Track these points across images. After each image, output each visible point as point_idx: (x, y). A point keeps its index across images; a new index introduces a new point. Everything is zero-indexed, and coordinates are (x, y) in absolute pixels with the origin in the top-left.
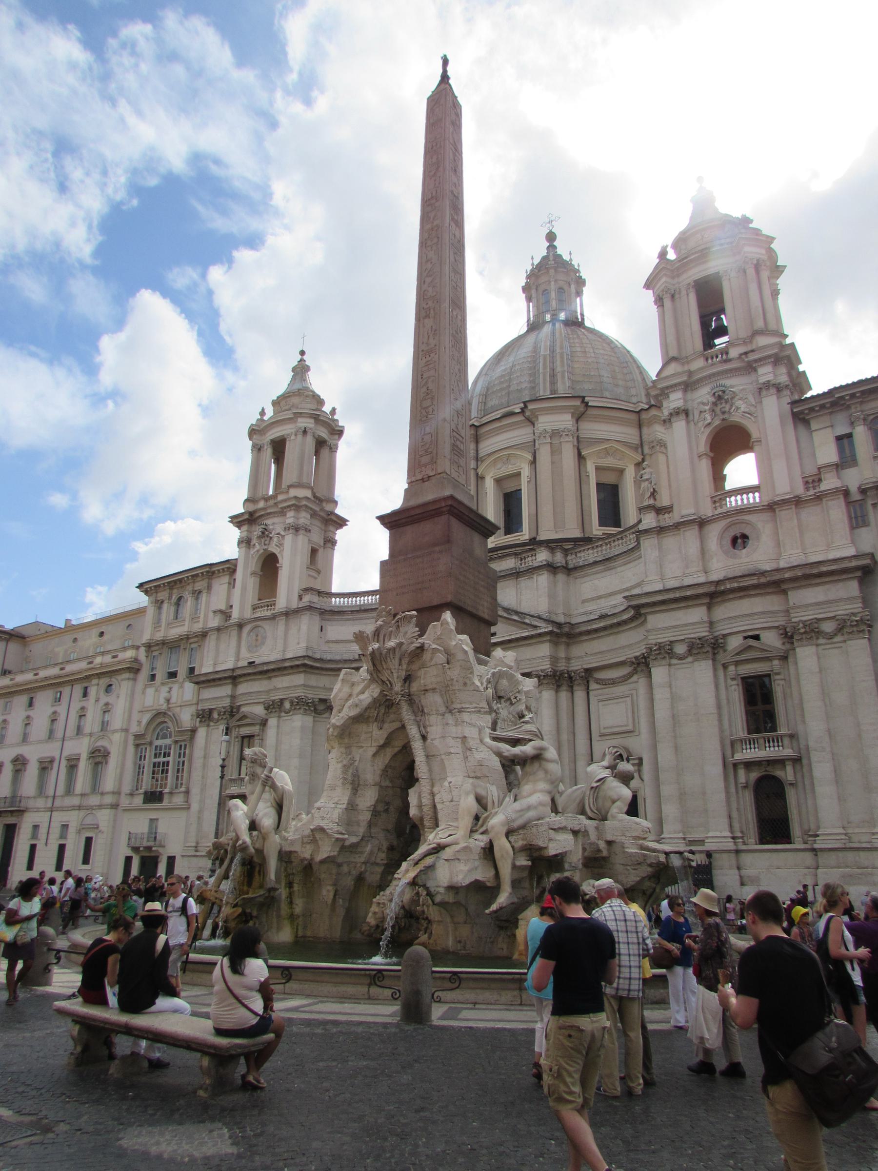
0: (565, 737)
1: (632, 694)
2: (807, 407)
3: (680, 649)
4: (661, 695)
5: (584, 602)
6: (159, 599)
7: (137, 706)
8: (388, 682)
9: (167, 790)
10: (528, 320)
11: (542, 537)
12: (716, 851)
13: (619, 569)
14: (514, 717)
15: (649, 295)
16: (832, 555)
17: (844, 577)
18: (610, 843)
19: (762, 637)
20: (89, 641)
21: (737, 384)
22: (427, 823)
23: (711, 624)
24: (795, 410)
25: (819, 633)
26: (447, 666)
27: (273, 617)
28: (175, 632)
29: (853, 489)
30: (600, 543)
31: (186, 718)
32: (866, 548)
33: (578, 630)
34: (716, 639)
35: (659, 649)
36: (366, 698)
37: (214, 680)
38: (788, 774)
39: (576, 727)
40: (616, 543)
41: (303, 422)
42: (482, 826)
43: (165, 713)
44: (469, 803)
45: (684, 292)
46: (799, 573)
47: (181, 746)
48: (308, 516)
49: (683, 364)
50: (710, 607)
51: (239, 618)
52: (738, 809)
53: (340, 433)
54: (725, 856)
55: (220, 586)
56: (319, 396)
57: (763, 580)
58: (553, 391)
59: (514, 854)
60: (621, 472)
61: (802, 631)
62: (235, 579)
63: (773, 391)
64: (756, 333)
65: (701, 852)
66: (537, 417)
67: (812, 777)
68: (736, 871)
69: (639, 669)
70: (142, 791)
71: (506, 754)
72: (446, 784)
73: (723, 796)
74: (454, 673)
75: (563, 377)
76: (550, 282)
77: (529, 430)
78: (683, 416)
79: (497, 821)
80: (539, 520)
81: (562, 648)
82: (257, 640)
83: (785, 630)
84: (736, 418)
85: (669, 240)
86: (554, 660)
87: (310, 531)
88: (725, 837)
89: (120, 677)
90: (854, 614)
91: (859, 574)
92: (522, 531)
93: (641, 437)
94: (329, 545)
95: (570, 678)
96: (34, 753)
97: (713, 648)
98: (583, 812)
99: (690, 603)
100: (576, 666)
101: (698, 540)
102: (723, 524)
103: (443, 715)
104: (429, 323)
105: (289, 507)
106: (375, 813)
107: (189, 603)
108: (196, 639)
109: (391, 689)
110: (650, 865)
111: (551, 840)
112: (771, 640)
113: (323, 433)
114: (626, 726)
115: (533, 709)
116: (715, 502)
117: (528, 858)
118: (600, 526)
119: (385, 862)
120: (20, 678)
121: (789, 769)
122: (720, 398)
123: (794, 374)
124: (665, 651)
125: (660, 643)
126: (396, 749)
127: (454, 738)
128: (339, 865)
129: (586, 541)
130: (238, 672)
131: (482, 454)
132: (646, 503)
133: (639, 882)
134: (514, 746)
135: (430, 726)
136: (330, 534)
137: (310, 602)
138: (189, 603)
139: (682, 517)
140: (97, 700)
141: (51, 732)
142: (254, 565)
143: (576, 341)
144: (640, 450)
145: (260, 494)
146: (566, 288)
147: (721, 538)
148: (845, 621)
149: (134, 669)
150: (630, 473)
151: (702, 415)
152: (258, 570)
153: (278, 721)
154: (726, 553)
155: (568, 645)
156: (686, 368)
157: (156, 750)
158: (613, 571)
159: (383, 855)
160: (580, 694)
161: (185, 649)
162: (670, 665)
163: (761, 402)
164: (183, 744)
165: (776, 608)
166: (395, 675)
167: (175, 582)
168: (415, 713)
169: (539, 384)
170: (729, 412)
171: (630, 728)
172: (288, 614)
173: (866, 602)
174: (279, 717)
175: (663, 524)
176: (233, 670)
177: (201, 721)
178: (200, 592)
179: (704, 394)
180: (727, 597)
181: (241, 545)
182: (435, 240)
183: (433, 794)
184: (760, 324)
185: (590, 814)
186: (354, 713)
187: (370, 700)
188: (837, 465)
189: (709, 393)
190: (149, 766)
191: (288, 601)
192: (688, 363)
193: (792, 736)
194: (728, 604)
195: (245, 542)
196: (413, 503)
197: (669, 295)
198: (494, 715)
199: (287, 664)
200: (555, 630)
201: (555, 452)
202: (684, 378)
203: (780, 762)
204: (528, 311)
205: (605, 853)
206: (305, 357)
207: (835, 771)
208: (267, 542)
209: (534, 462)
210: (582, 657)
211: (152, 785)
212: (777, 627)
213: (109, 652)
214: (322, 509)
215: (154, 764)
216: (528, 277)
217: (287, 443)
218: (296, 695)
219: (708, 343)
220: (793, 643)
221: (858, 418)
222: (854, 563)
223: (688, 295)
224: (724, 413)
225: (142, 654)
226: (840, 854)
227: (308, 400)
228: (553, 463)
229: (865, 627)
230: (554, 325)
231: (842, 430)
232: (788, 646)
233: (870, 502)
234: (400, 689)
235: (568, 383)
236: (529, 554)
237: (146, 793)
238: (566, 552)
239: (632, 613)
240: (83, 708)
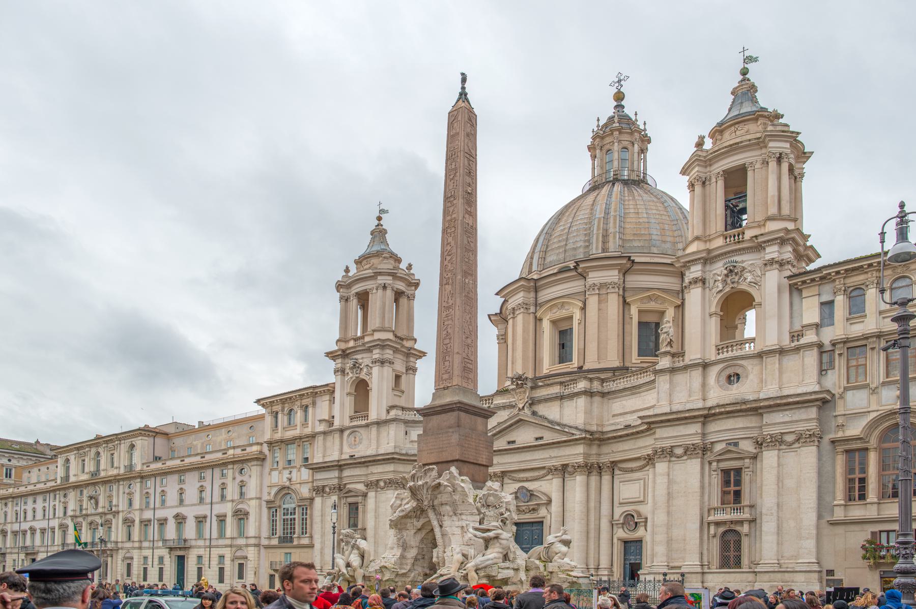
108: (307, 439)
129: (623, 370)
134: (484, 533)
161: (299, 446)
213: (238, 447)
225: (265, 449)
236: (572, 382)
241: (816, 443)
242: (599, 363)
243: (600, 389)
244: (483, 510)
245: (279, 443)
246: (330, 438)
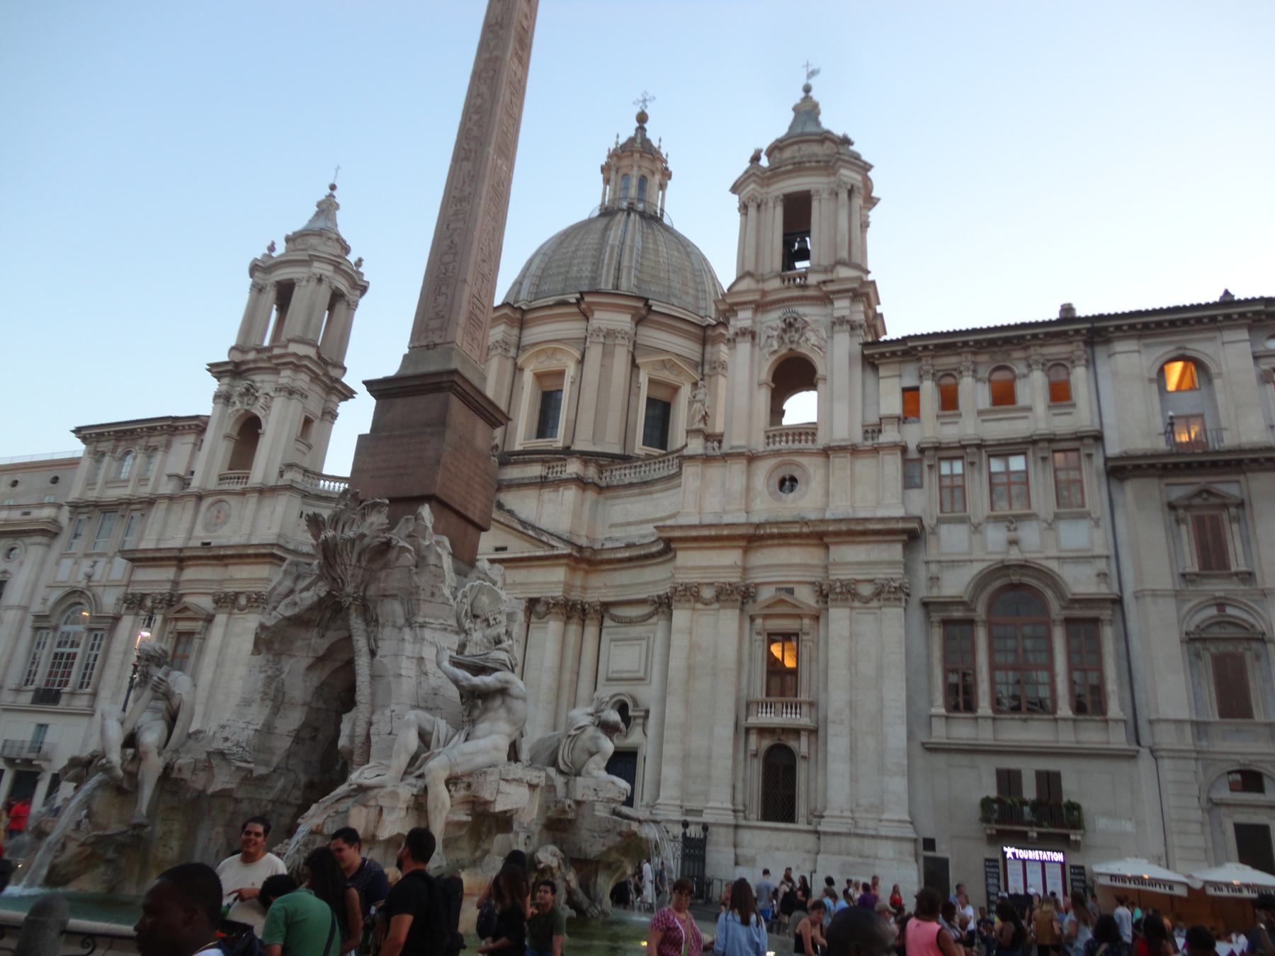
1: (649, 638)
2: (878, 351)
3: (708, 593)
4: (679, 641)
5: (612, 526)
6: (100, 449)
8: (339, 581)
9: (67, 689)
10: (603, 203)
11: (578, 446)
12: (714, 824)
13: (655, 496)
14: (490, 642)
15: (734, 200)
16: (880, 513)
17: (889, 538)
18: (579, 803)
21: (809, 312)
22: (356, 758)
23: (745, 570)
24: (865, 352)
25: (855, 595)
26: (414, 570)
27: (243, 493)
28: (113, 494)
29: (912, 446)
30: (639, 463)
31: (109, 601)
32: (916, 511)
33: (599, 557)
34: (747, 587)
35: (685, 590)
36: (309, 597)
37: (154, 559)
38: (802, 746)
39: (583, 666)
40: (657, 466)
41: (319, 268)
42: (420, 767)
43: (82, 592)
44: (411, 741)
45: (771, 204)
46: (844, 527)
47: (96, 636)
48: (307, 379)
49: (758, 281)
50: (746, 551)
51: (199, 488)
52: (744, 780)
53: (363, 289)
54: (722, 831)
55: (182, 446)
56: (345, 242)
57: (805, 530)
58: (617, 287)
59: (452, 806)
60: (675, 389)
61: (838, 590)
62: (202, 440)
63: (847, 327)
64: (840, 263)
65: (697, 823)
66: (592, 312)
67: (826, 751)
68: (732, 850)
69: (660, 610)
70: (33, 687)
71: (465, 683)
72: (388, 712)
73: (729, 763)
74: (423, 581)
75: (629, 273)
76: (632, 166)
77: (582, 324)
78: (749, 338)
79: (437, 768)
80: (577, 427)
81: (580, 574)
82: (218, 517)
83: (821, 586)
84: (804, 350)
85: (765, 145)
86: (568, 587)
87: (306, 397)
88: (725, 809)
89: (28, 540)
90: (892, 580)
91: (905, 537)
92: (553, 435)
93: (703, 355)
94: (328, 417)
95: (584, 610)
97: (743, 597)
98: (554, 763)
99: (726, 544)
101: (745, 476)
102: (773, 462)
103: (400, 629)
104: (467, 166)
105: (285, 364)
106: (298, 738)
107: (138, 460)
108: (138, 506)
109: (342, 590)
110: (620, 834)
111: (498, 792)
112: (806, 596)
113: (342, 285)
114: (638, 671)
115: (514, 635)
116: (768, 437)
117: (468, 812)
118: (644, 444)
119: (299, 802)
121: (804, 739)
122: (790, 325)
123: (871, 314)
124: (690, 593)
125: (686, 584)
126: (338, 664)
127: (408, 657)
128: (237, 801)
130: (187, 553)
131: (526, 341)
132: (695, 427)
133: (603, 854)
135: (383, 639)
136: (331, 405)
137: (292, 481)
139: (732, 448)
142: (230, 427)
143: (650, 236)
144: (700, 369)
145: (253, 342)
146: (649, 176)
147: (769, 477)
149: (50, 532)
150: (685, 392)
151: (769, 341)
152: (235, 434)
153: (229, 618)
154: (771, 494)
155: (587, 572)
156: (761, 286)
157: (61, 637)
158: (648, 497)
159: (297, 793)
160: (591, 630)
161: (123, 516)
163: (832, 338)
164: (99, 633)
165: (815, 561)
166: (350, 572)
167: (125, 432)
168: (367, 623)
169: (601, 275)
170: (798, 343)
171: (641, 674)
172: (263, 491)
173: (908, 568)
174: (230, 614)
175: (710, 452)
176: (181, 550)
177: (127, 608)
178: (155, 449)
179: (774, 318)
180: (764, 543)
181: (218, 400)
182: (491, 73)
183: (370, 724)
184: (843, 254)
185: (562, 767)
186: (288, 613)
187: (315, 598)
188: (899, 418)
189: (780, 318)
190: (48, 656)
191: (265, 475)
192: (763, 281)
193: (812, 705)
194: (766, 551)
195: (222, 398)
196: (410, 372)
197: (755, 205)
198: (463, 636)
199: (251, 551)
200: (575, 553)
201: (607, 354)
202: (757, 297)
203: (796, 732)
204: (604, 194)
205: (571, 816)
206: (335, 193)
207: (851, 748)
208: (251, 402)
209: (581, 362)
210: (600, 588)
211: (47, 682)
212: (813, 583)
213: (18, 506)
214: (326, 374)
215: (56, 654)
216: (610, 157)
217: (296, 288)
218: (257, 590)
219: (788, 263)
220: (827, 603)
221: (928, 372)
222: (901, 525)
223: (774, 208)
224: (792, 342)
225: (64, 516)
226: (844, 840)
227: (330, 243)
228: (602, 366)
229: (903, 597)
230: (629, 215)
231: (910, 382)
232: (821, 605)
233: (926, 463)
234: (352, 591)
235: (633, 281)
237: (37, 690)
238: (601, 470)
239: (661, 546)
242: (594, 444)
243: (597, 480)
244: (468, 624)
245: (91, 509)
246: (177, 507)
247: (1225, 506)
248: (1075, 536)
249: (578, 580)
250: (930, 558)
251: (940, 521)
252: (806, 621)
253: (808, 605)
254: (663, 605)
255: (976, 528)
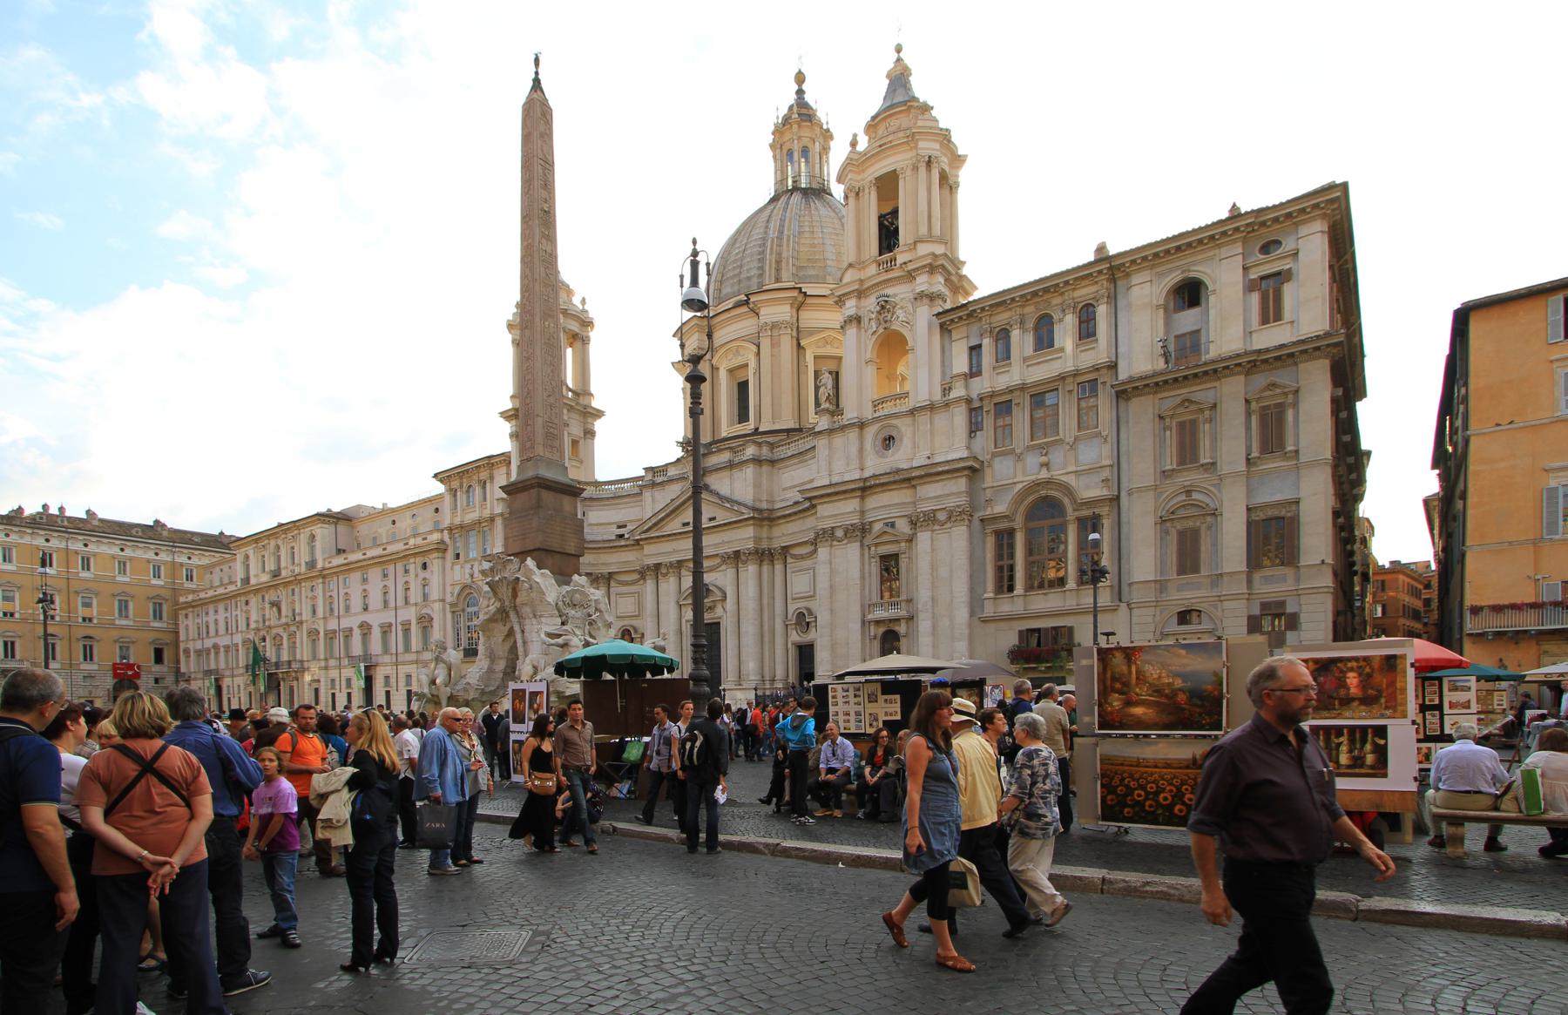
0: (765, 601)
3: (840, 533)
4: (823, 571)
5: (784, 489)
7: (449, 581)
13: (810, 462)
19: (897, 525)
20: (405, 523)
23: (862, 513)
28: (471, 517)
33: (774, 516)
50: (862, 498)
57: (897, 478)
81: (765, 529)
86: (757, 539)
89: (431, 557)
96: (376, 620)
99: (847, 496)
100: (777, 544)
112: (903, 527)
116: (875, 406)
120: (353, 557)
124: (827, 535)
138: (478, 490)
140: (417, 576)
141: (386, 603)
148: (952, 512)
149: (441, 548)
154: (877, 452)
155: (771, 527)
160: (779, 567)
162: (831, 546)
173: (971, 493)
194: (875, 497)
209: (758, 354)
225: (446, 538)
228: (772, 356)
238: (772, 446)
240: (407, 582)
241: (967, 522)
247: (1201, 410)
248: (1094, 453)
249: (764, 533)
250: (986, 486)
251: (994, 455)
252: (903, 544)
253: (904, 534)
254: (814, 543)
255: (1019, 458)
